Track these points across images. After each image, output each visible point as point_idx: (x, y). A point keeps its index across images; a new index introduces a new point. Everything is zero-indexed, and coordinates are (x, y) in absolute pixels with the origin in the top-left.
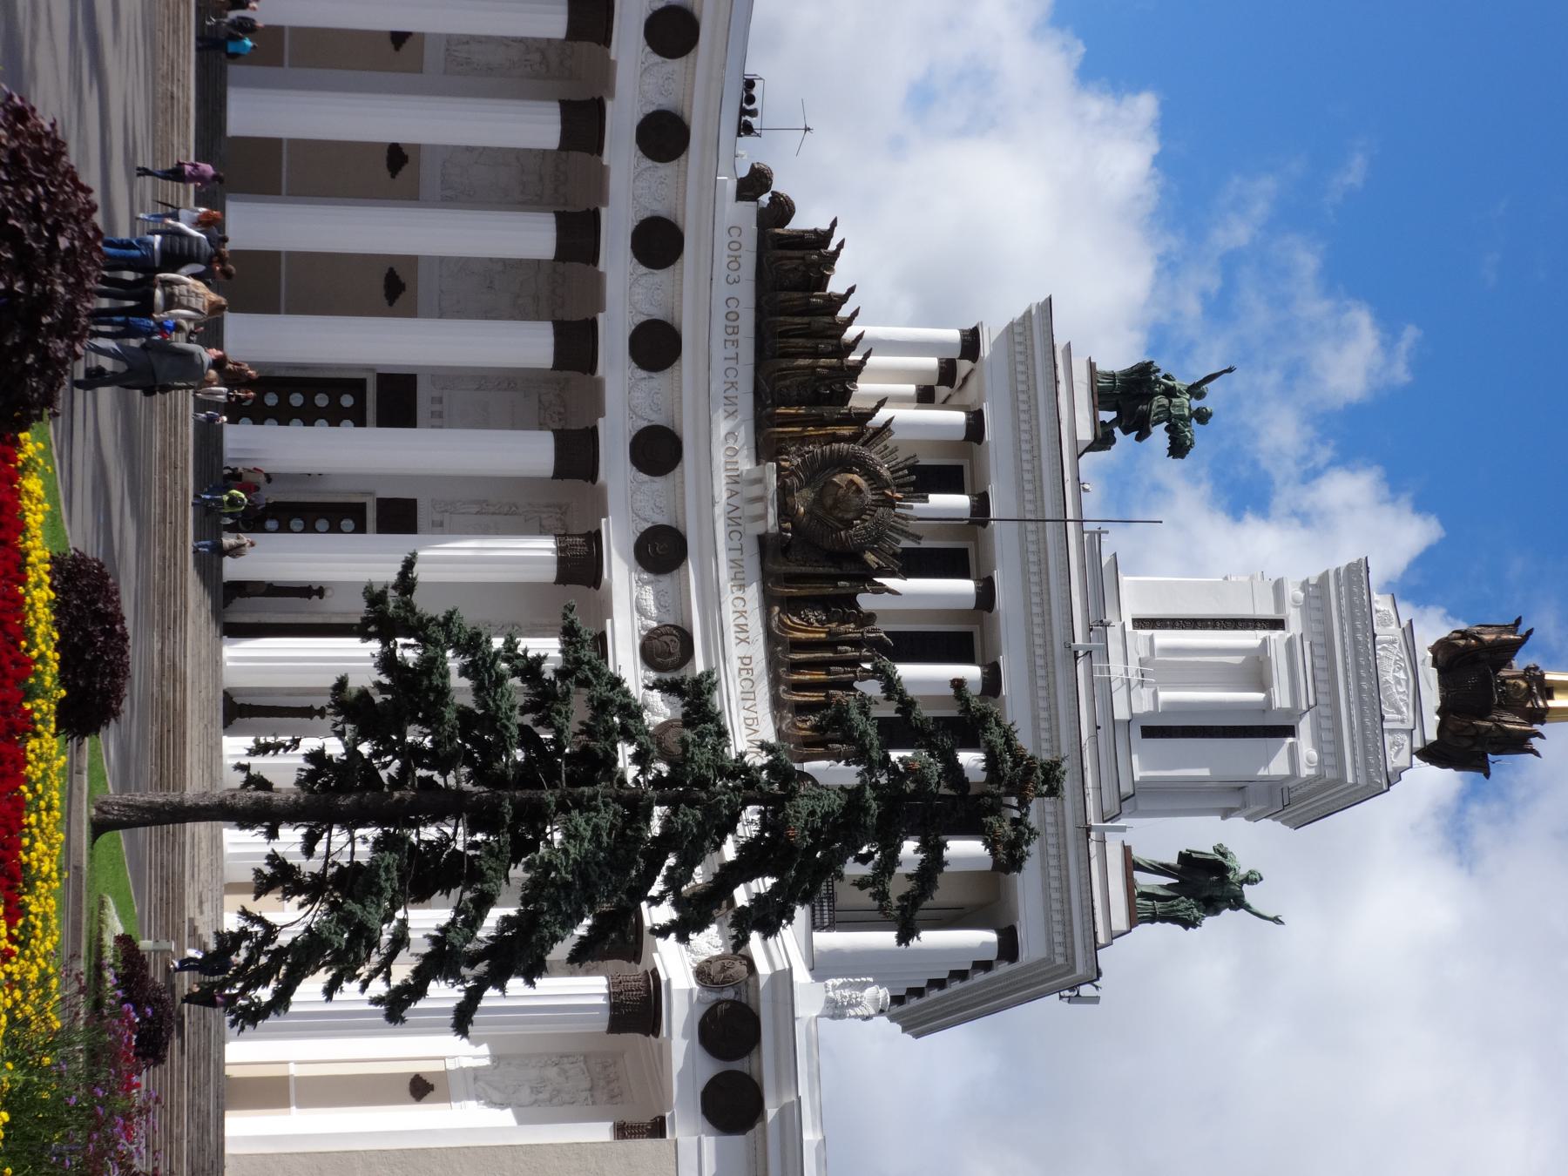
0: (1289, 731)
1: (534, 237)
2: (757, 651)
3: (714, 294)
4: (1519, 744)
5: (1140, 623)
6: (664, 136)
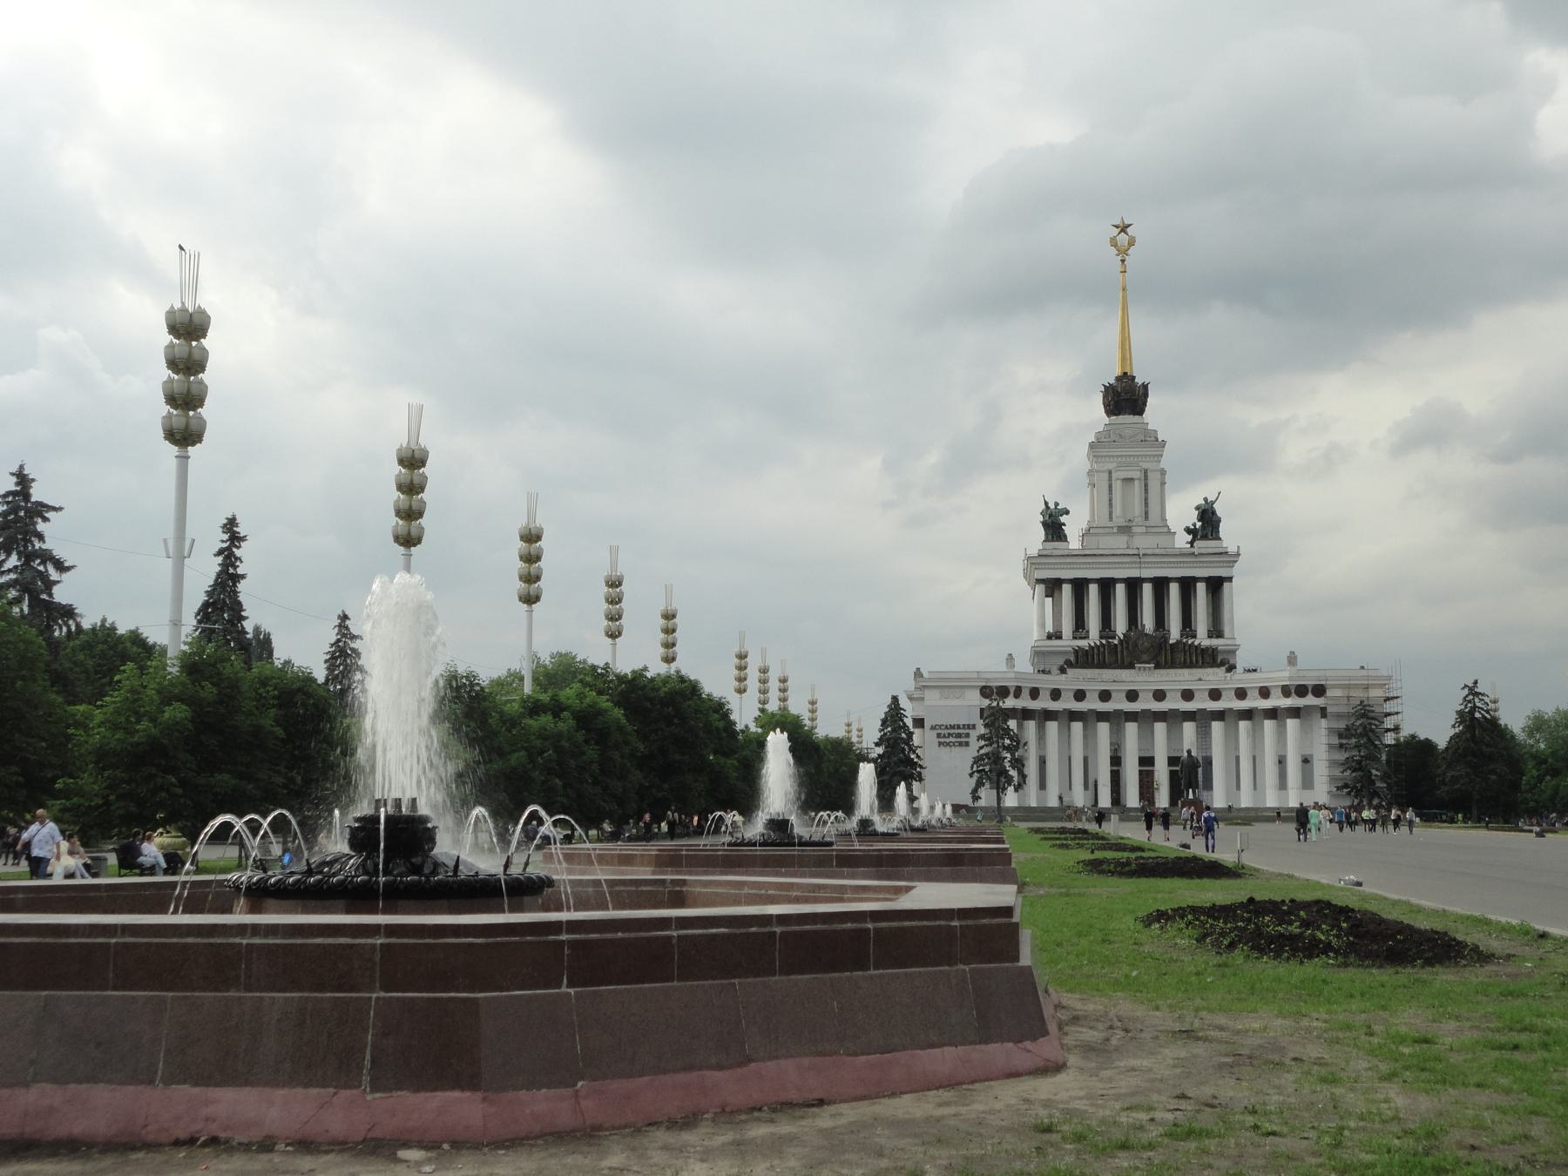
0: (1146, 472)
1: (1077, 727)
2: (1186, 671)
3: (1093, 679)
4: (1145, 387)
5: (1111, 519)
6: (1056, 694)
